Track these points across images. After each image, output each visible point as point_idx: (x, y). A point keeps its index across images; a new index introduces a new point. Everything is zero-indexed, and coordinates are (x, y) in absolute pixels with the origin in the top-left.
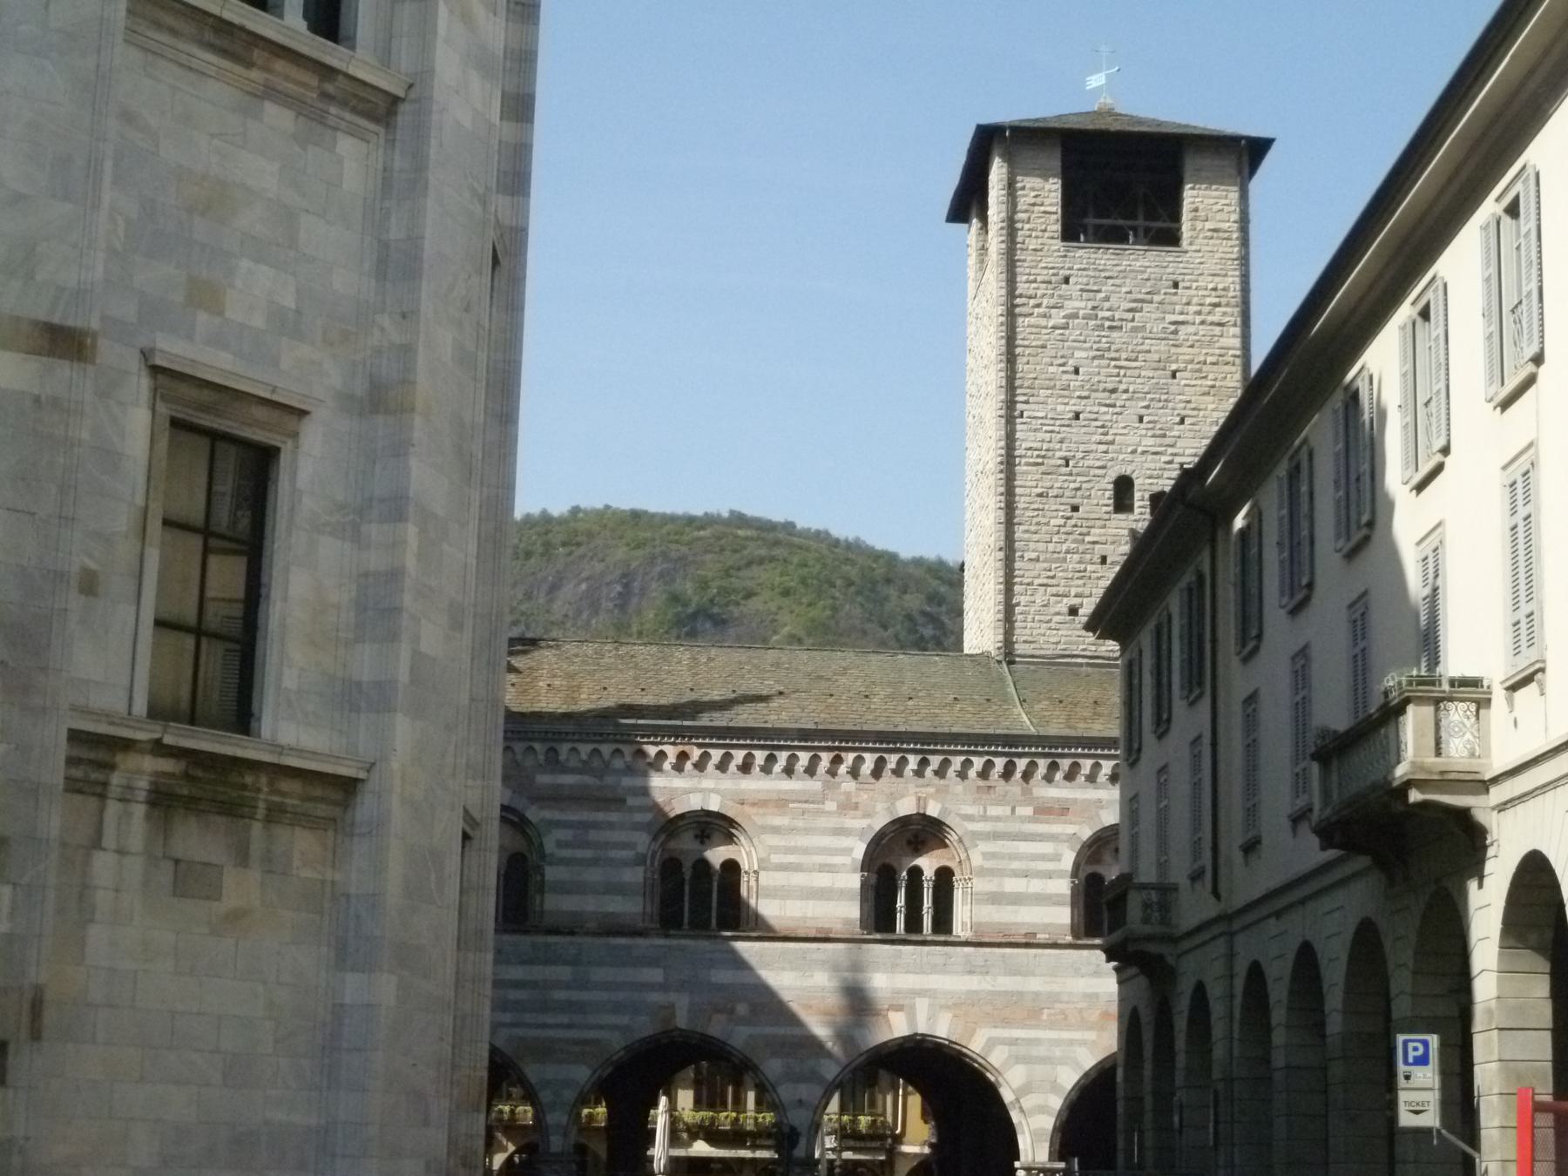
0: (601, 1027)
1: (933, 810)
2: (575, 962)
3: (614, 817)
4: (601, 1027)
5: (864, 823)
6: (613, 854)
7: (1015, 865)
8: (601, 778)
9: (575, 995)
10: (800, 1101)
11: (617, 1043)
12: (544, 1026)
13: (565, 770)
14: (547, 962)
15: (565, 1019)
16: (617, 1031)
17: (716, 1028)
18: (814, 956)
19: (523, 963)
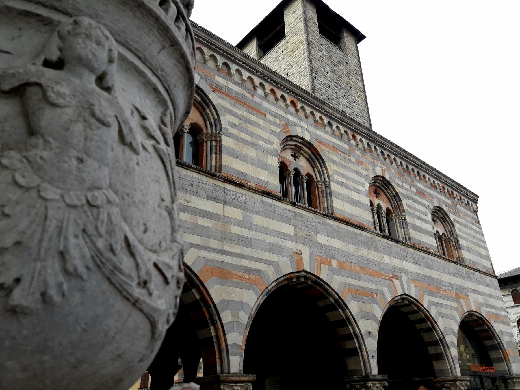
0: (262, 261)
1: (387, 177)
2: (244, 208)
3: (261, 122)
4: (262, 261)
5: (365, 173)
6: (261, 143)
7: (417, 213)
8: (253, 95)
9: (246, 233)
10: (370, 333)
11: (272, 276)
12: (223, 252)
13: (232, 81)
14: (225, 202)
15: (237, 249)
16: (276, 267)
17: (324, 275)
18: (360, 238)
19: (209, 198)
